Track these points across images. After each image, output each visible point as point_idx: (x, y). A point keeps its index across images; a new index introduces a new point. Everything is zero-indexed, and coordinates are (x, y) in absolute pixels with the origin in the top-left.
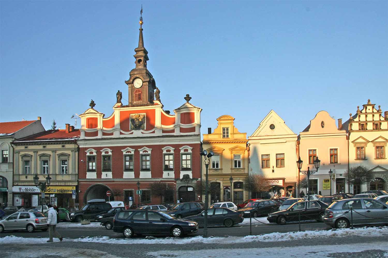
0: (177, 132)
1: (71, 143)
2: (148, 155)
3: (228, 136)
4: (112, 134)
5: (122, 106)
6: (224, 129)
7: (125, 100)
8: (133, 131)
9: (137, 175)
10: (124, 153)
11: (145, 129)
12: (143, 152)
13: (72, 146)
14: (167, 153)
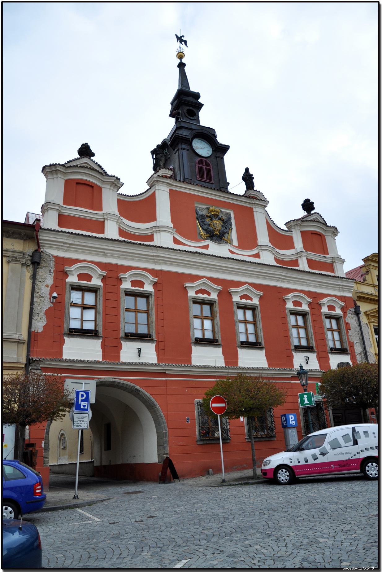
1: (13, 233)
10: (191, 293)
12: (242, 297)
14: (295, 307)
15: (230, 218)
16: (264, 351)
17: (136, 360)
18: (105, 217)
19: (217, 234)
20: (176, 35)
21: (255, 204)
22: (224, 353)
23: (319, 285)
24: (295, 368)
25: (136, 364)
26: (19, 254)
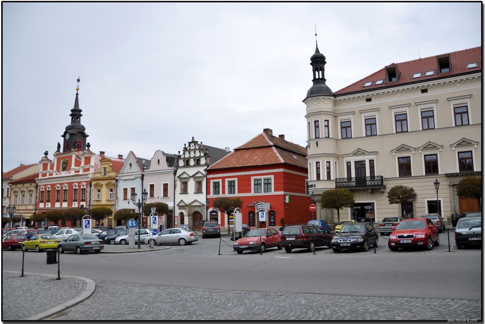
0: (81, 173)
7: (62, 150)
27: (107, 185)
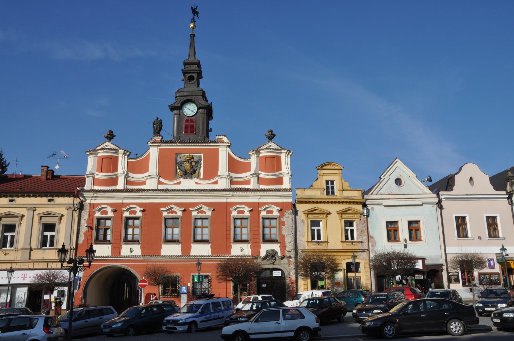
2: (206, 218)
3: (333, 193)
4: (144, 183)
5: (162, 142)
6: (327, 182)
8: (182, 180)
9: (186, 250)
11: (202, 177)
13: (68, 200)
14: (238, 215)
15: (200, 160)
16: (210, 245)
17: (129, 254)
18: (118, 175)
19: (189, 173)
20: (192, 8)
21: (220, 145)
22: (182, 248)
23: (260, 197)
24: (231, 254)
25: (128, 257)
26: (71, 205)
27: (343, 213)
